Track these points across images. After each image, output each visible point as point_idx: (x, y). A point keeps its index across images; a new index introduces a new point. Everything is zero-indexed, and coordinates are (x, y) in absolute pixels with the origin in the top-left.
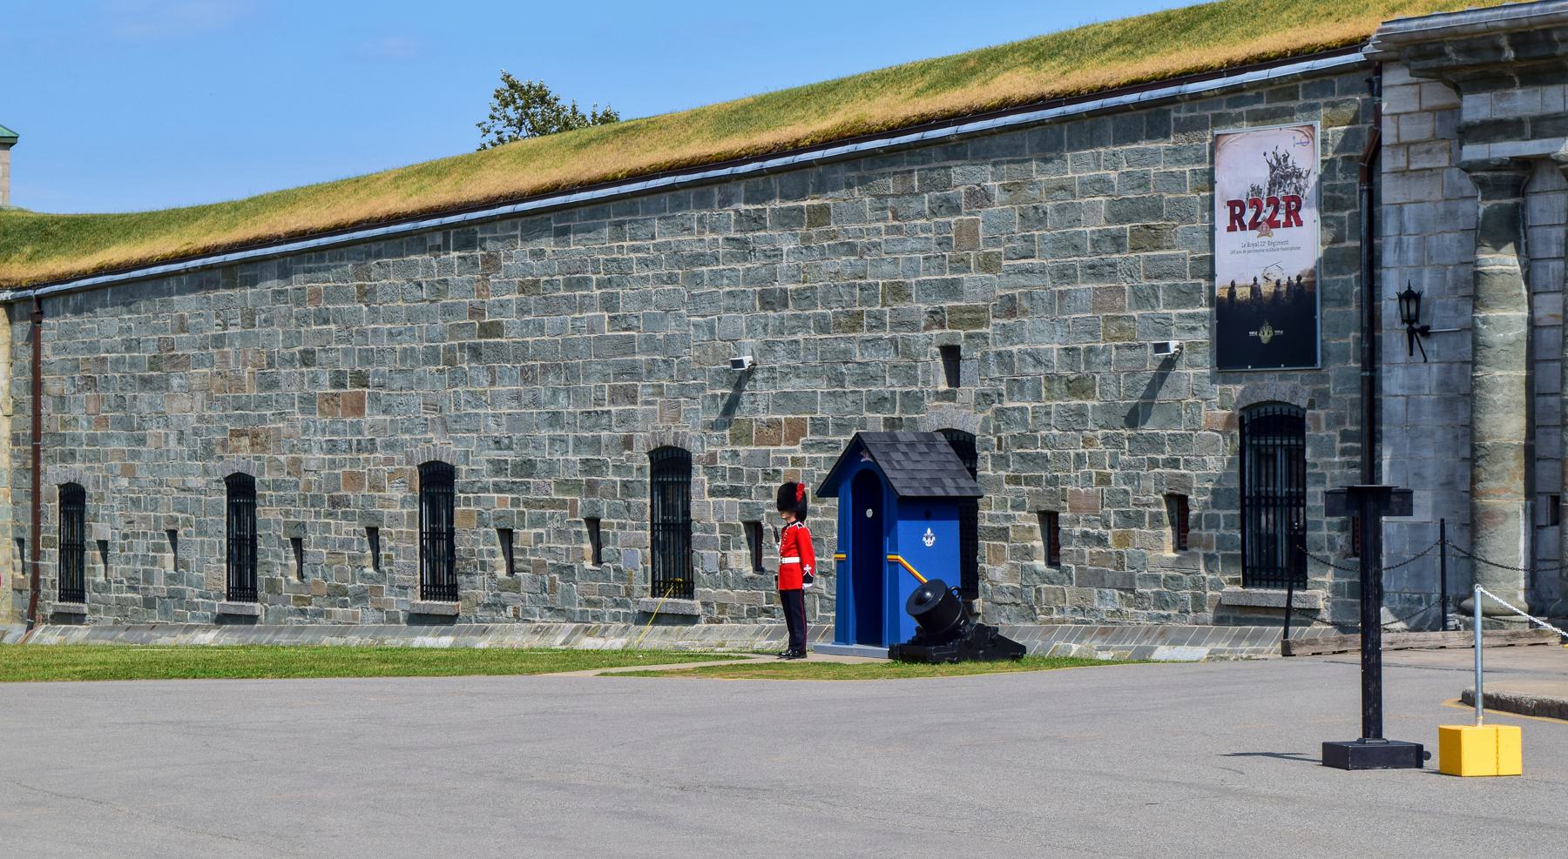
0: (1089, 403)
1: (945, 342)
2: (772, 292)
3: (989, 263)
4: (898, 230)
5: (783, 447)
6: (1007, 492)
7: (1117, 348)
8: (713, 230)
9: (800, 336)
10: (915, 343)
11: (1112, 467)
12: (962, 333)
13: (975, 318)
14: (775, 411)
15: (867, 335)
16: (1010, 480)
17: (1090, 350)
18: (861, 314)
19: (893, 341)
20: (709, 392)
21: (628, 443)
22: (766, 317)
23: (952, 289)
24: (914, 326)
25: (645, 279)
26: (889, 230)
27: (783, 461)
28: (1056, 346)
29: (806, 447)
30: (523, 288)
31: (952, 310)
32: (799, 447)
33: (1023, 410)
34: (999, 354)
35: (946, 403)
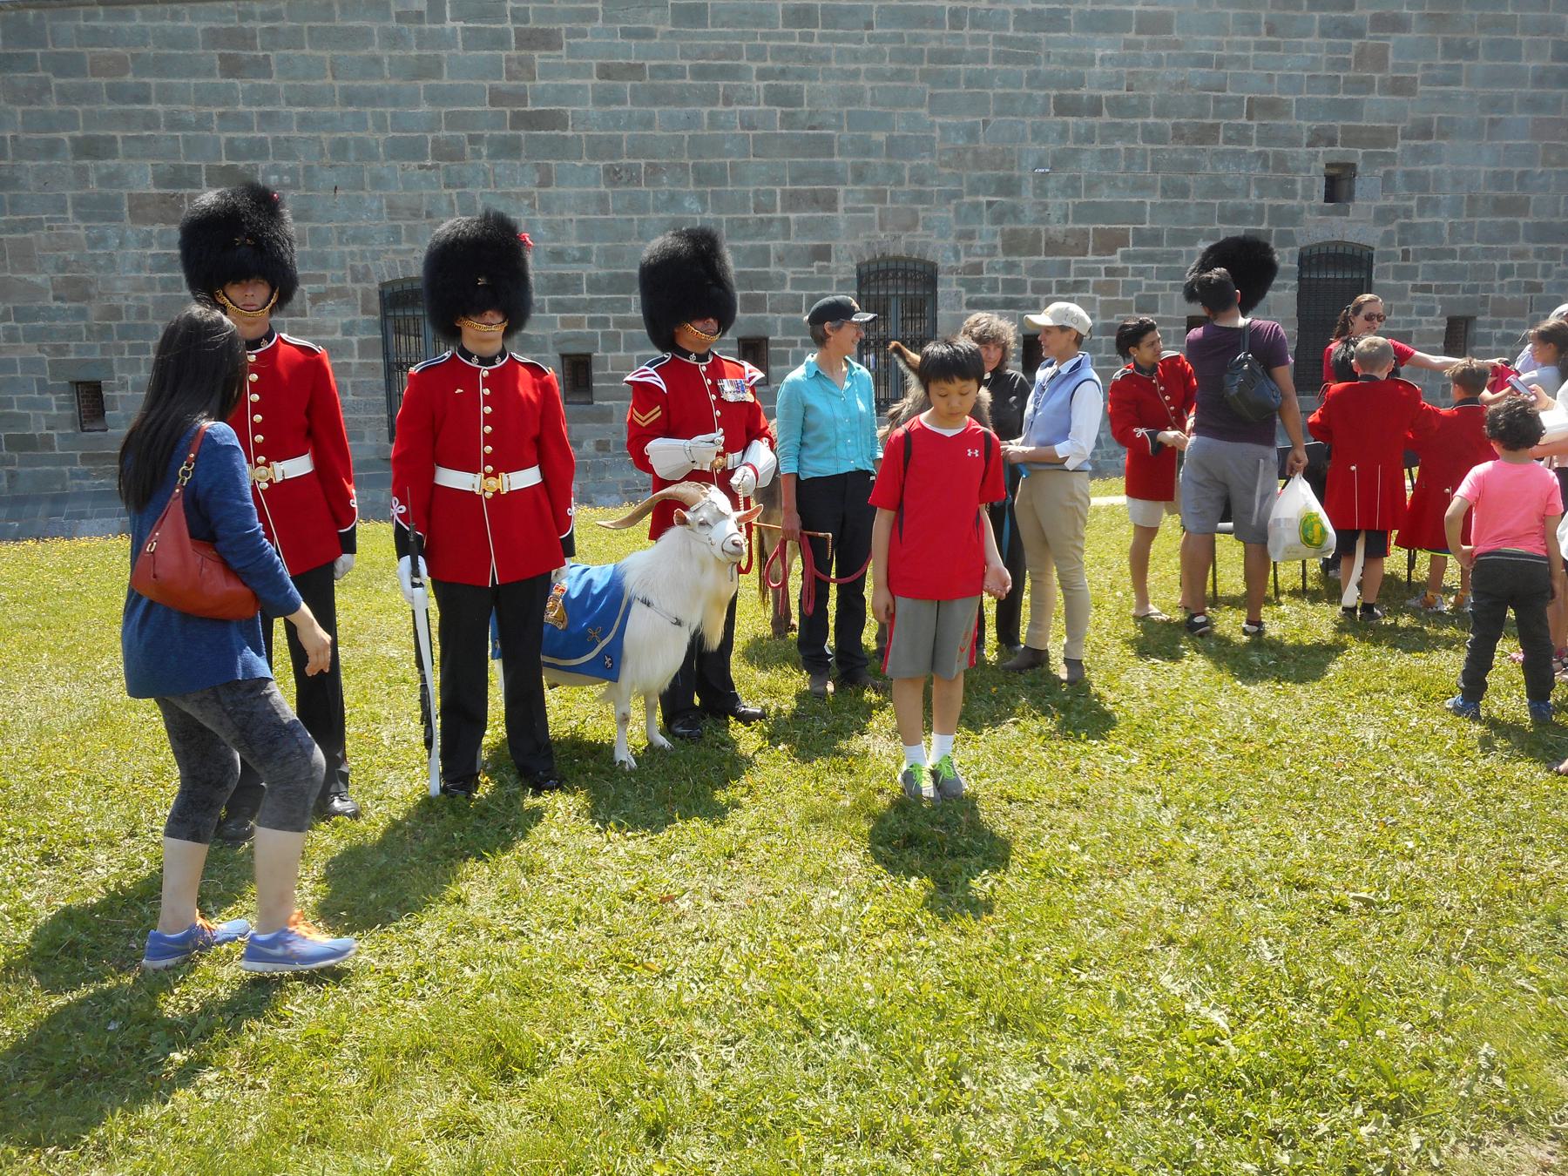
0: (1521, 221)
1: (1335, 159)
2: (1079, 98)
3: (1400, 87)
4: (1275, 47)
5: (1090, 257)
6: (1414, 299)
7: (1557, 173)
8: (975, 25)
9: (1119, 145)
10: (1293, 159)
11: (1545, 276)
12: (1360, 151)
13: (1380, 138)
14: (1076, 221)
15: (1221, 147)
16: (1415, 288)
17: (1523, 175)
18: (1215, 127)
19: (1259, 154)
20: (967, 199)
21: (822, 253)
22: (1066, 124)
23: (1350, 109)
24: (1294, 143)
25: (855, 74)
26: (1259, 46)
27: (1096, 272)
28: (1483, 169)
29: (1126, 257)
30: (605, 72)
31: (1346, 130)
32: (1118, 256)
33: (1437, 227)
34: (1408, 175)
35: (1335, 219)
